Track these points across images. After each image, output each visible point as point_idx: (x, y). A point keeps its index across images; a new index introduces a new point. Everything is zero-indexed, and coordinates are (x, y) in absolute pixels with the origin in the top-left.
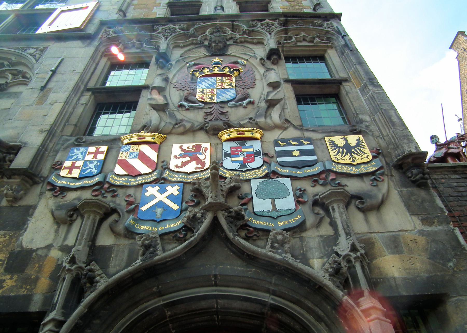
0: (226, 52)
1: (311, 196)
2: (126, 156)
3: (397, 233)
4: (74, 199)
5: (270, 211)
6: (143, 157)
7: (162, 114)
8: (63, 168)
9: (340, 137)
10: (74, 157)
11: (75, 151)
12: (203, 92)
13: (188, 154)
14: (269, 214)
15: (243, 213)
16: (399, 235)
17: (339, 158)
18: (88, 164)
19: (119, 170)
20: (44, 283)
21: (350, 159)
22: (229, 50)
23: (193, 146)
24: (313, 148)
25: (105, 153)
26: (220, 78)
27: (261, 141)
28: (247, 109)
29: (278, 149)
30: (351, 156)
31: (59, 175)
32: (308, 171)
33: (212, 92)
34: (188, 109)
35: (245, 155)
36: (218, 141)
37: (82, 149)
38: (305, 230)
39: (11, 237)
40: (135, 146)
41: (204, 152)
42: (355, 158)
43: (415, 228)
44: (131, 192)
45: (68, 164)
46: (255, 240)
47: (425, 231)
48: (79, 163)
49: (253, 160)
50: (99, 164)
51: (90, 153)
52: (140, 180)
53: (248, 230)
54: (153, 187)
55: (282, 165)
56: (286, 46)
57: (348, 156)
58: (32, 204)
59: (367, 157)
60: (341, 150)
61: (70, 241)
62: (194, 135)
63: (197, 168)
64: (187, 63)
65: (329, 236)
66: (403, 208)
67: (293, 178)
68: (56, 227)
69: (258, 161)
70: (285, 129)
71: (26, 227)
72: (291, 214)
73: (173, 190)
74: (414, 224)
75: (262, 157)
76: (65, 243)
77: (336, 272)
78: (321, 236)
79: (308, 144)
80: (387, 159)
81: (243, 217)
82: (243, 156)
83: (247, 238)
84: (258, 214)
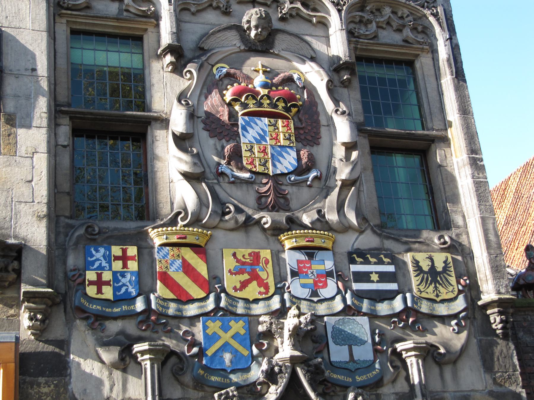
0: (271, 49)
1: (389, 342)
2: (167, 267)
3: (469, 393)
4: (118, 334)
5: (347, 362)
8: (87, 283)
9: (425, 255)
10: (97, 264)
11: (94, 252)
12: (251, 150)
13: (243, 267)
14: (347, 366)
15: (323, 367)
16: (469, 396)
17: (422, 290)
18: (120, 278)
21: (434, 291)
22: (277, 42)
23: (250, 255)
24: (394, 270)
25: (137, 258)
26: (272, 120)
27: (334, 254)
28: (313, 189)
29: (354, 268)
30: (436, 287)
31: (86, 294)
33: (264, 151)
34: (233, 183)
35: (316, 275)
36: (279, 247)
37: (102, 250)
38: (382, 386)
39: (56, 386)
40: (175, 249)
41: (264, 265)
42: (439, 291)
43: (486, 387)
45: (91, 276)
46: (332, 396)
47: (494, 392)
48: (107, 276)
49: (325, 285)
50: (134, 278)
51: (117, 258)
53: (326, 385)
54: (214, 321)
56: (362, 42)
57: (432, 288)
58: (62, 338)
59: (452, 292)
60: (426, 276)
62: (247, 232)
63: (260, 293)
64: (213, 66)
65: (404, 394)
66: (480, 363)
68: (107, 373)
69: (330, 288)
70: (361, 232)
71: (69, 371)
74: (486, 383)
75: (335, 280)
76: (127, 396)
78: (396, 394)
79: (389, 264)
80: (472, 294)
81: (323, 372)
82: (313, 277)
84: (335, 365)
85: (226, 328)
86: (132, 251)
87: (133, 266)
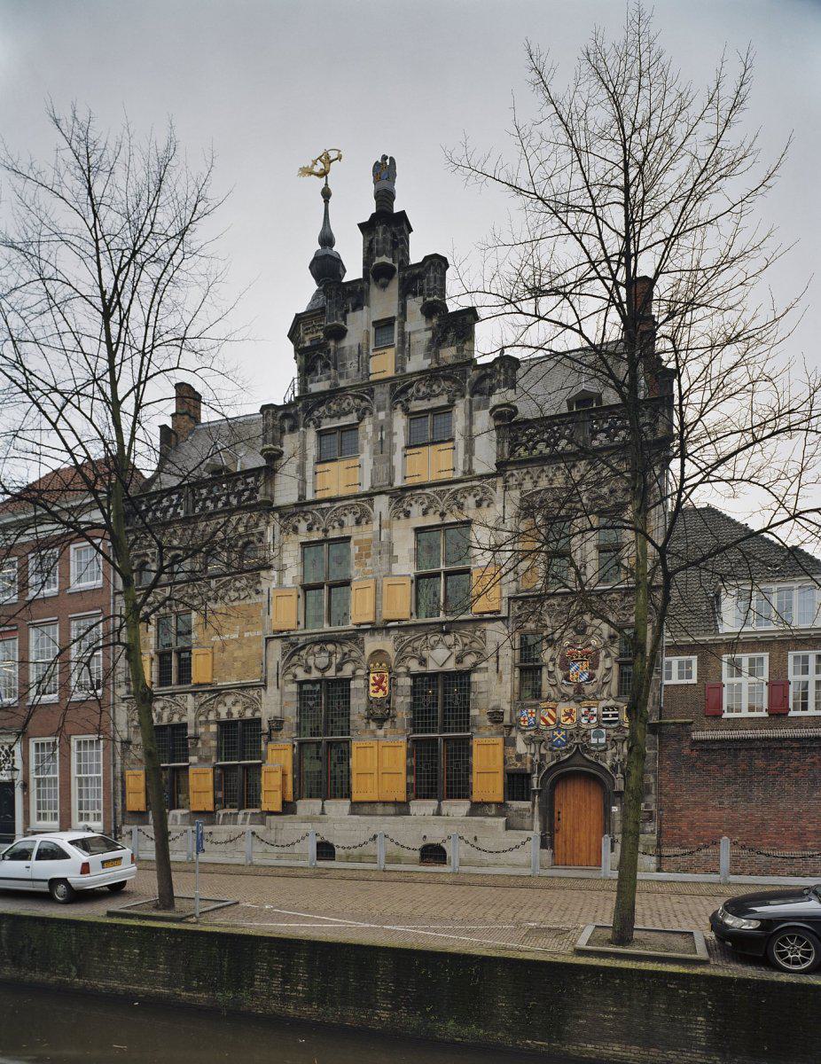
6: (550, 715)
7: (555, 688)
19: (543, 723)
20: (529, 765)
32: (613, 725)
44: (548, 732)
45: (522, 719)
48: (527, 719)
52: (552, 727)
55: (605, 722)
61: (533, 752)
67: (606, 729)
69: (595, 719)
72: (603, 745)
73: (563, 733)
77: (612, 767)
83: (588, 753)
85: (559, 733)
86: (534, 711)
87: (534, 715)
